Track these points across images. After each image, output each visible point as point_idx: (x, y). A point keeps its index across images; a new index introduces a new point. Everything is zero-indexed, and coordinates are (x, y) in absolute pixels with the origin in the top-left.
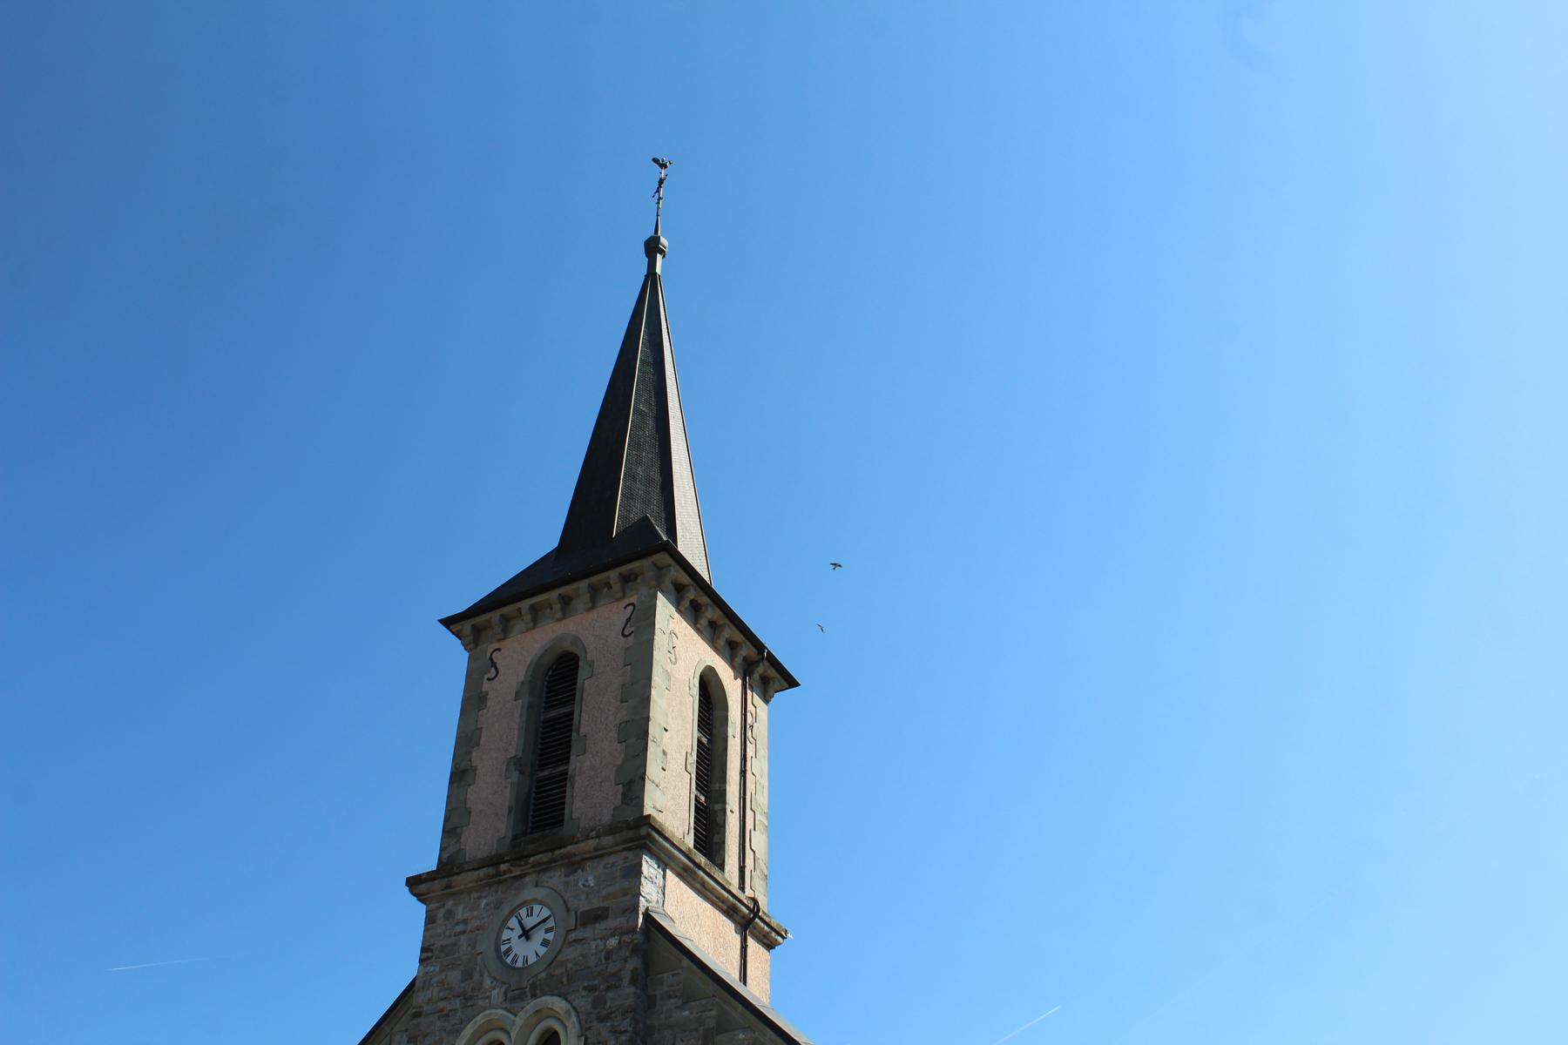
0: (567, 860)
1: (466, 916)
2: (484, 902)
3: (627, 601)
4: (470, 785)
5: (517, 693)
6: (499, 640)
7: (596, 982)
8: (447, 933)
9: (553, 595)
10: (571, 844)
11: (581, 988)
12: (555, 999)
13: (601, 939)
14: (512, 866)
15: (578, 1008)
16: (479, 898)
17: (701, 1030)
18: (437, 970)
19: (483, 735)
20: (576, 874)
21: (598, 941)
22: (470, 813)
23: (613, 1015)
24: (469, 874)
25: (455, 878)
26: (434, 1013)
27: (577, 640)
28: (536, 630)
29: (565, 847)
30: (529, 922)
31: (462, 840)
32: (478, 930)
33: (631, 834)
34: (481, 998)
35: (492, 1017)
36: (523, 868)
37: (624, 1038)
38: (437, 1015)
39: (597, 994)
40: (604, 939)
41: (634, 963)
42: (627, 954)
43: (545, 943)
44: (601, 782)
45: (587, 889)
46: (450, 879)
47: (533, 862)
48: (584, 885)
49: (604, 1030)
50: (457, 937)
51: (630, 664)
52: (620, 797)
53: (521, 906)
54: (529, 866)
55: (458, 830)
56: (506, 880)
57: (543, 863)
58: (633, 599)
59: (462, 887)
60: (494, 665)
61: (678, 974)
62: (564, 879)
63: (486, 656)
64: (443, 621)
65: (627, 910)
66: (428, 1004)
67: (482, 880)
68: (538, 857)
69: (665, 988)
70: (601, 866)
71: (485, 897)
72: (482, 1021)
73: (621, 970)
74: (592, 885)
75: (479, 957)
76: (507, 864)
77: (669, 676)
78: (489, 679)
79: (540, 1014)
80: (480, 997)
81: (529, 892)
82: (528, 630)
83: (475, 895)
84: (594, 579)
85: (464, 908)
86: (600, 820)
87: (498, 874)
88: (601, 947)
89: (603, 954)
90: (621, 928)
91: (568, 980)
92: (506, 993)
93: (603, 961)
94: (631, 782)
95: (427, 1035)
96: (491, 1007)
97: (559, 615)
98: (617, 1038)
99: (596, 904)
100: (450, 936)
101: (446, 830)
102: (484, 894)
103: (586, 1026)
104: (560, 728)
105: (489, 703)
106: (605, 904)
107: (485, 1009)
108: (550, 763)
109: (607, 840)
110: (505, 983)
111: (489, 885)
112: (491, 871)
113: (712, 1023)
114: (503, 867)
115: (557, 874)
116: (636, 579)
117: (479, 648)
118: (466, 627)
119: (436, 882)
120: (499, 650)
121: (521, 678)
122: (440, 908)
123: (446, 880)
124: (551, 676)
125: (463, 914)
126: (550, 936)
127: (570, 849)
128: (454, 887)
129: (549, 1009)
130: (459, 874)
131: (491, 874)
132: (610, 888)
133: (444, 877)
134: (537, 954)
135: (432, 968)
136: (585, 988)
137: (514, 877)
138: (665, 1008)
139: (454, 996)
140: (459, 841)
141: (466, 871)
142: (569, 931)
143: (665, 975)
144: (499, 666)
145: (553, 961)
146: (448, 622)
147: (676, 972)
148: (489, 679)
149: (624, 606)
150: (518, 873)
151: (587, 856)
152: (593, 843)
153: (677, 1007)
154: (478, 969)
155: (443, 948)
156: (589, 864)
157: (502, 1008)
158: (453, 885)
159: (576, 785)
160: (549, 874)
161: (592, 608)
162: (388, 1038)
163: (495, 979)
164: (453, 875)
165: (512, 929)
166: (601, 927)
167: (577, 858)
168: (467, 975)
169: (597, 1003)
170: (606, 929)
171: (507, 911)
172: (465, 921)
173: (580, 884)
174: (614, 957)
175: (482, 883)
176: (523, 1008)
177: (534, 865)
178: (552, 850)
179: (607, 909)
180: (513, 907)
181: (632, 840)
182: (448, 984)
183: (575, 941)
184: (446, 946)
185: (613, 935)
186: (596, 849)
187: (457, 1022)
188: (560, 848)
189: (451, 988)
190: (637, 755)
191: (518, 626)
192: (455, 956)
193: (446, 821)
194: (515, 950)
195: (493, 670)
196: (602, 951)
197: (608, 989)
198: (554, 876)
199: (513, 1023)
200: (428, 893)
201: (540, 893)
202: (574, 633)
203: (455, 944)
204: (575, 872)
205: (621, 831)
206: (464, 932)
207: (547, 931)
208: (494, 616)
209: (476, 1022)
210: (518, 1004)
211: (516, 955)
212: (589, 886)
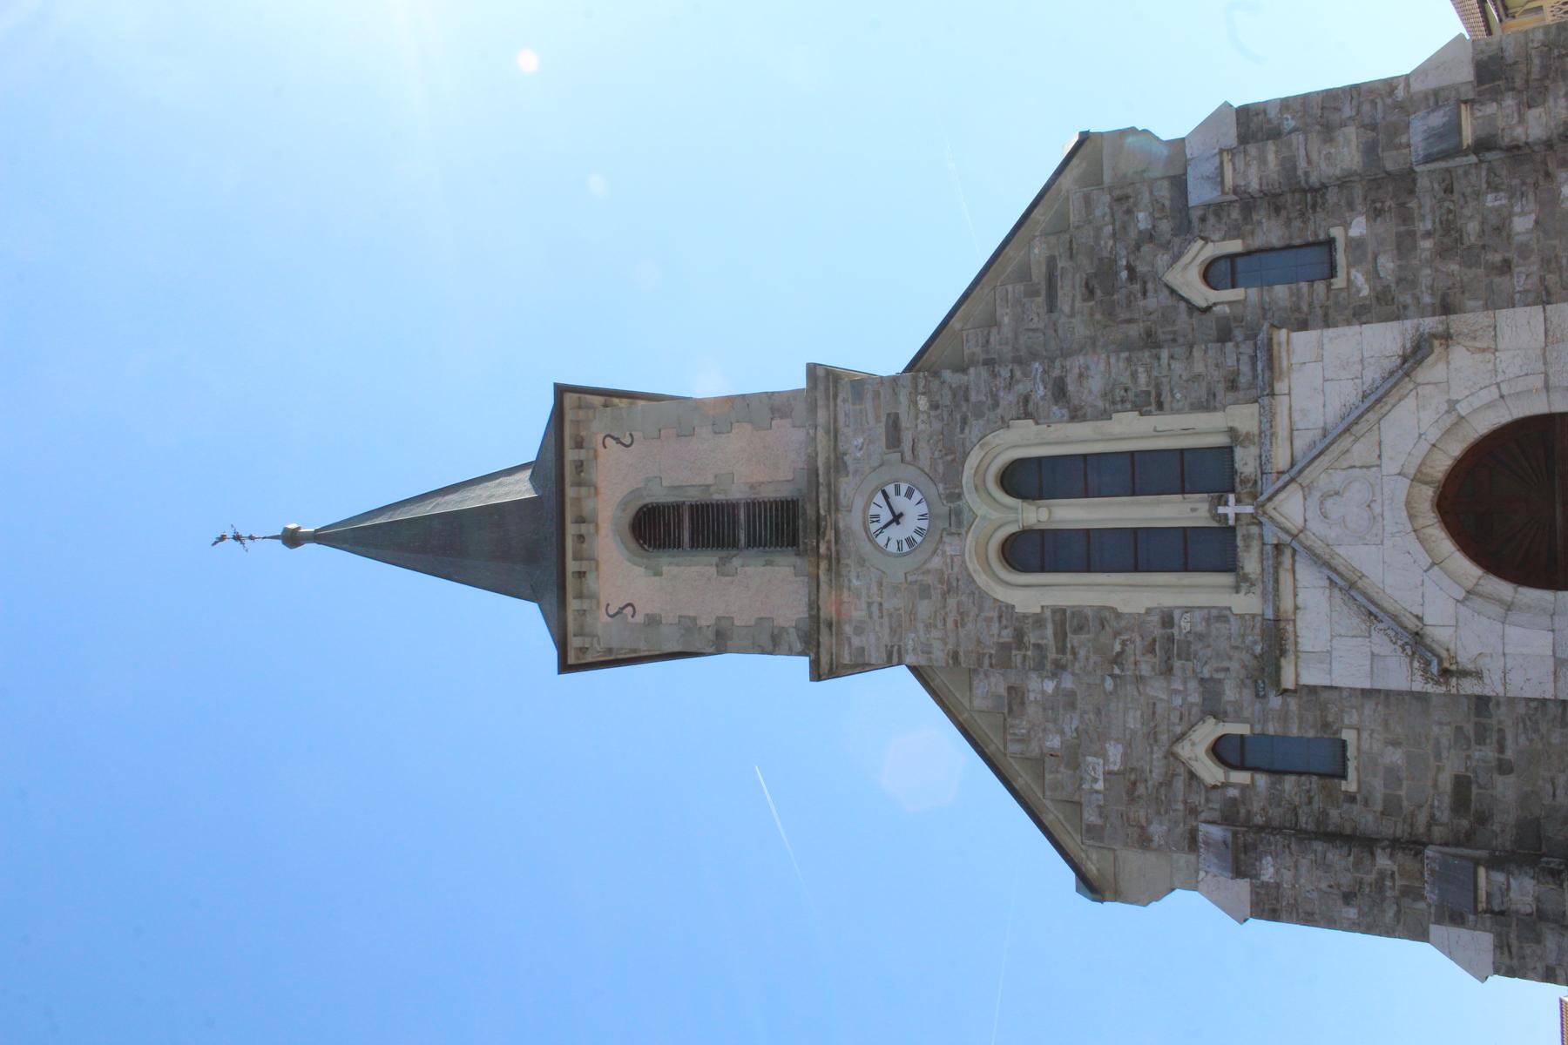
0: (832, 471)
1: (864, 606)
3: (600, 447)
4: (733, 622)
5: (655, 575)
7: (958, 417)
8: (877, 628)
9: (571, 529)
10: (816, 461)
11: (962, 436)
12: (967, 466)
13: (917, 418)
15: (980, 435)
16: (849, 589)
17: (1024, 300)
18: (913, 635)
19: (684, 613)
20: (848, 463)
21: (919, 420)
22: (761, 619)
23: (994, 389)
24: (821, 595)
25: (822, 614)
26: (957, 634)
27: (624, 504)
29: (817, 470)
30: (886, 516)
32: (881, 585)
33: (821, 387)
34: (952, 569)
35: (973, 552)
36: (829, 528)
37: (1018, 374)
38: (960, 629)
39: (969, 414)
40: (918, 412)
41: (947, 375)
42: (937, 382)
43: (909, 494)
45: (865, 447)
46: (821, 621)
47: (825, 511)
48: (861, 449)
49: (1007, 399)
50: (885, 613)
51: (660, 431)
53: (867, 530)
54: (828, 517)
55: (776, 631)
56: (838, 553)
57: (829, 499)
61: (967, 336)
62: (850, 477)
66: (946, 644)
67: (831, 580)
68: (821, 504)
69: (978, 350)
71: (849, 580)
72: (976, 562)
73: (951, 387)
74: (862, 440)
75: (909, 578)
76: (821, 545)
78: (633, 616)
79: (980, 487)
80: (950, 571)
81: (852, 521)
84: (568, 479)
89: (932, 413)
90: (910, 393)
91: (952, 453)
92: (951, 534)
93: (939, 411)
94: (772, 409)
95: (979, 642)
96: (963, 554)
97: (592, 528)
98: (1018, 382)
99: (881, 430)
100: (881, 625)
102: (846, 583)
103: (1000, 423)
104: (703, 523)
105: (657, 611)
106: (884, 419)
107: (964, 562)
108: (734, 529)
109: (822, 416)
110: (941, 537)
111: (838, 574)
112: (823, 565)
113: (1020, 288)
114: (823, 550)
117: (600, 633)
119: (821, 640)
120: (608, 605)
121: (642, 570)
122: (850, 644)
123: (823, 628)
124: (649, 546)
125: (862, 610)
126: (904, 488)
128: (831, 618)
129: (975, 475)
130: (819, 609)
131: (827, 566)
133: (818, 627)
135: (911, 642)
136: (962, 430)
137: (836, 542)
138: (998, 347)
139: (945, 607)
143: (967, 351)
145: (929, 476)
147: (965, 338)
148: (633, 616)
149: (603, 448)
150: (833, 535)
151: (832, 443)
153: (999, 333)
154: (921, 577)
155: (893, 631)
156: (841, 448)
157: (965, 540)
159: (761, 480)
160: (842, 496)
162: (974, 714)
163: (934, 552)
164: (818, 618)
165: (889, 540)
166: (905, 421)
167: (832, 456)
168: (925, 592)
169: (979, 415)
171: (868, 547)
172: (869, 605)
174: (937, 398)
175: (834, 581)
176: (971, 509)
177: (829, 511)
179: (889, 415)
180: (866, 539)
181: (827, 390)
182: (930, 618)
184: (891, 628)
185: (916, 403)
186: (828, 432)
187: (970, 601)
188: (817, 475)
189: (935, 612)
190: (748, 405)
191: (588, 506)
193: (763, 652)
194: (910, 533)
195: (625, 611)
197: (967, 400)
199: (984, 518)
200: (832, 655)
201: (858, 505)
203: (890, 616)
204: (845, 463)
205: (816, 400)
206: (881, 604)
207: (898, 493)
208: (573, 604)
209: (975, 571)
210: (966, 516)
211: (916, 531)
212: (863, 444)
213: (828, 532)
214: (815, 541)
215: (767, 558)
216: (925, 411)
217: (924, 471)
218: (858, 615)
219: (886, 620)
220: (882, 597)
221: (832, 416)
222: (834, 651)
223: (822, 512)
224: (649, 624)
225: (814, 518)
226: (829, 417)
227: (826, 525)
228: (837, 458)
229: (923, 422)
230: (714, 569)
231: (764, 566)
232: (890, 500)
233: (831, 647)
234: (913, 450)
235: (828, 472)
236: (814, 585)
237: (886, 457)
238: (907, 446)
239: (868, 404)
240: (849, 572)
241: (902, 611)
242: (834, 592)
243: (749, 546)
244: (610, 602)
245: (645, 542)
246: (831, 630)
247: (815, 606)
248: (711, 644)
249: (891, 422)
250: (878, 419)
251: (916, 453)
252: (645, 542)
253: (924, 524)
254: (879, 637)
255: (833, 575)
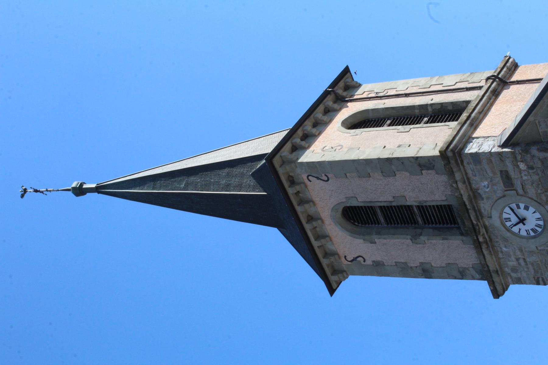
0: (473, 200)
1: (514, 259)
2: (504, 249)
4: (432, 266)
5: (372, 243)
6: (340, 258)
8: (526, 270)
9: (308, 227)
10: (462, 199)
13: (521, 173)
14: (480, 234)
16: (502, 252)
19: (399, 261)
20: (481, 193)
21: (523, 175)
22: (449, 264)
25: (491, 269)
28: (330, 235)
29: (464, 203)
30: (514, 219)
31: (467, 267)
32: (522, 251)
33: (452, 162)
40: (520, 171)
41: (534, 151)
42: (529, 156)
43: (527, 208)
44: (421, 184)
45: (490, 186)
46: (491, 271)
47: (476, 221)
48: (488, 187)
50: (528, 263)
51: (345, 174)
52: (430, 171)
53: (504, 226)
54: (479, 223)
55: (461, 270)
56: (489, 237)
57: (476, 215)
58: (305, 177)
59: (496, 264)
60: (355, 259)
61: (539, 122)
62: (485, 201)
63: (350, 265)
64: (331, 295)
65: (500, 159)
67: (490, 252)
68: (472, 218)
70: (474, 178)
71: (501, 248)
73: (539, 159)
75: (539, 248)
76: (479, 238)
77: (351, 149)
78: (364, 261)
81: (495, 221)
82: (331, 240)
83: (500, 255)
84: (295, 203)
85: (509, 261)
86: (445, 182)
87: (486, 242)
88: (526, 173)
89: (531, 171)
90: (512, 161)
93: (535, 170)
94: (420, 165)
97: (319, 222)
99: (498, 179)
100: (528, 268)
101: (460, 277)
104: (390, 213)
106: (499, 173)
109: (458, 176)
111: (493, 247)
112: (484, 247)
114: (481, 239)
115: (482, 205)
116: (292, 177)
117: (345, 269)
118: (333, 279)
119: (494, 280)
120: (345, 257)
121: (362, 241)
122: (511, 276)
123: (493, 275)
124: (359, 223)
125: (513, 261)
126: (522, 206)
127: (465, 199)
128: (497, 268)
130: (488, 266)
131: (486, 246)
132: (488, 171)
133: (491, 276)
134: (534, 212)
137: (487, 232)
140: (467, 269)
141: (486, 261)
142: (518, 194)
143: (540, 131)
144: (355, 256)
146: (332, 291)
147: (538, 124)
148: (364, 261)
149: (309, 182)
150: (484, 230)
151: (469, 187)
152: (460, 185)
155: (536, 272)
156: (474, 186)
158: (495, 270)
159: (425, 199)
160: (483, 211)
161: (313, 202)
164: (489, 270)
165: (520, 230)
166: (513, 174)
170: (514, 171)
171: (508, 234)
172: (517, 260)
173: (487, 190)
174: (532, 164)
177: (478, 220)
178: (467, 210)
179: (501, 171)
180: (506, 231)
181: (456, 161)
183: (523, 190)
184: (534, 269)
185: (518, 166)
186: (464, 182)
188: (465, 205)
190: (402, 163)
191: (330, 247)
192: (540, 263)
193: (455, 278)
194: (533, 226)
196: (529, 173)
198: (484, 207)
201: (495, 215)
202: (330, 211)
203: (532, 264)
204: (479, 194)
205: (452, 168)
206: (524, 259)
207: (519, 207)
208: (325, 262)
211: (536, 226)
213: (481, 231)
214: (475, 237)
215: (442, 237)
216: (525, 170)
217: (532, 199)
218: (512, 263)
219: (530, 266)
220: (524, 256)
221: (464, 173)
222: (503, 282)
223: (475, 222)
224: (376, 266)
225: (471, 226)
226: (462, 175)
227: (479, 228)
228: (473, 192)
229: (525, 175)
230: (409, 241)
231: (442, 240)
232: (515, 211)
233: (501, 281)
234: (523, 189)
235: (471, 201)
236: (482, 257)
237: (506, 193)
238: (518, 184)
239: (487, 167)
240: (499, 244)
241: (539, 262)
242: (494, 257)
243: (425, 224)
244: (346, 255)
245: (355, 221)
246: (498, 274)
247: (485, 266)
248: (420, 275)
249: (504, 176)
250: (494, 173)
251: (525, 190)
252: (355, 221)
253: (541, 223)
254: (528, 274)
255: (491, 249)
